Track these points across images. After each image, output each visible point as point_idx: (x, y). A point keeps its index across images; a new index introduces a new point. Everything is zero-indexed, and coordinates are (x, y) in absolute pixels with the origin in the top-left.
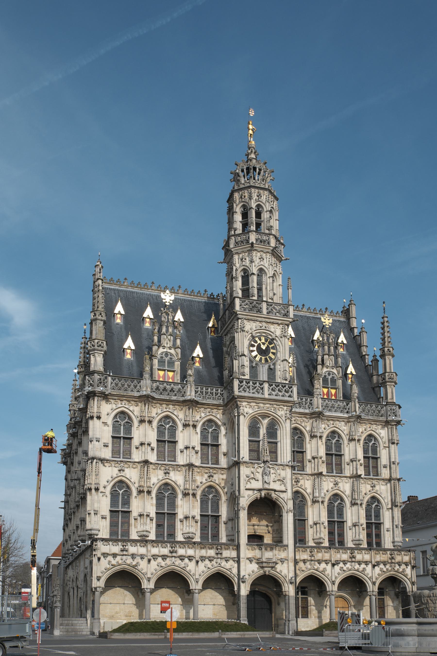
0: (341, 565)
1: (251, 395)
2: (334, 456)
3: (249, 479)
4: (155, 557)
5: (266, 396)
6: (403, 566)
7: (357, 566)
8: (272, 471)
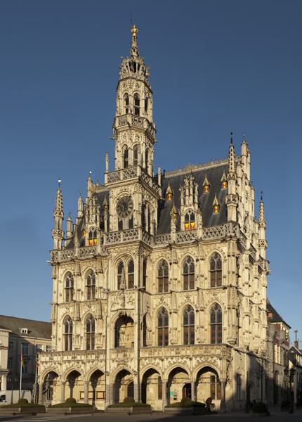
0: (169, 359)
1: (114, 243)
2: (189, 273)
3: (113, 304)
4: (65, 362)
5: (121, 242)
6: (215, 358)
7: (180, 360)
8: (126, 296)
